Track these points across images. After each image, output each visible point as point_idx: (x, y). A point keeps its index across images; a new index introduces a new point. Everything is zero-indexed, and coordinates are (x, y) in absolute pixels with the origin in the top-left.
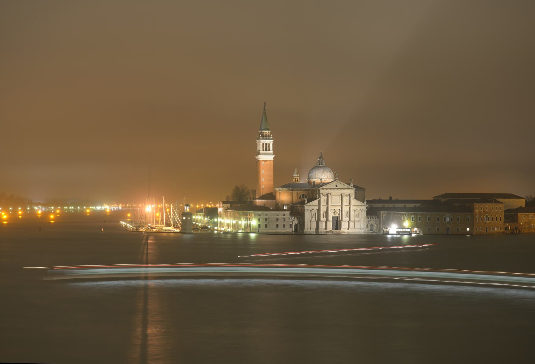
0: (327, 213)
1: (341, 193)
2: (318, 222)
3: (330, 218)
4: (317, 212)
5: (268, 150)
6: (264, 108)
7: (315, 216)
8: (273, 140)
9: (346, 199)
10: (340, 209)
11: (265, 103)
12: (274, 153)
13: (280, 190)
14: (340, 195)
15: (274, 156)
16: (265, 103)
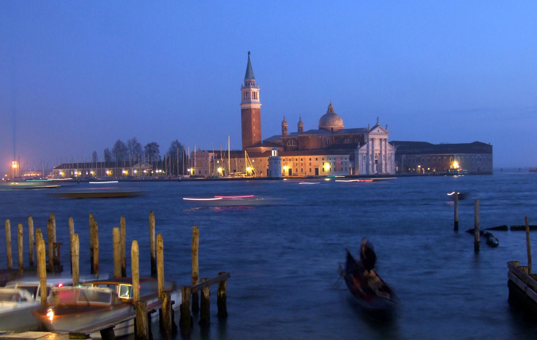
0: (372, 155)
1: (381, 138)
2: (367, 165)
3: (375, 162)
4: (365, 156)
5: (256, 98)
6: (249, 57)
7: (365, 159)
8: (259, 89)
9: (383, 143)
10: (379, 152)
11: (249, 53)
12: (261, 102)
13: (309, 136)
14: (379, 139)
16: (249, 53)
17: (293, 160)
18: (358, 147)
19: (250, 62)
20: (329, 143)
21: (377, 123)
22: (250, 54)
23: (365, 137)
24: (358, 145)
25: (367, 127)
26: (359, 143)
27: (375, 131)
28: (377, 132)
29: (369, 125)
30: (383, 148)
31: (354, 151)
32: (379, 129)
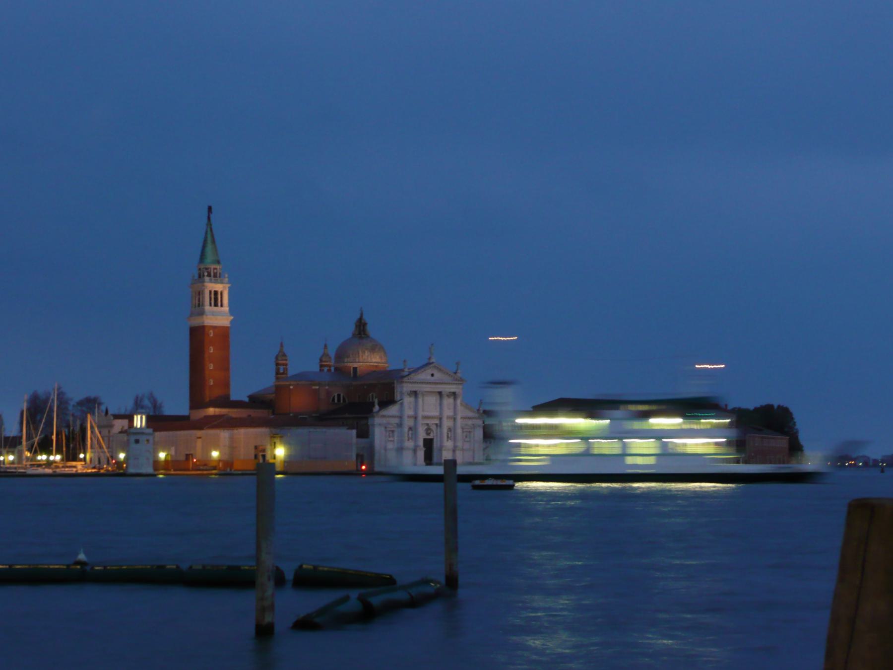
3: (421, 443)
5: (219, 304)
6: (209, 218)
7: (393, 436)
8: (229, 285)
11: (210, 208)
12: (232, 311)
15: (232, 317)
16: (210, 208)
20: (342, 401)
22: (213, 210)
25: (401, 367)
26: (376, 401)
27: (425, 375)
28: (429, 377)
30: (448, 412)
31: (367, 418)
32: (435, 372)
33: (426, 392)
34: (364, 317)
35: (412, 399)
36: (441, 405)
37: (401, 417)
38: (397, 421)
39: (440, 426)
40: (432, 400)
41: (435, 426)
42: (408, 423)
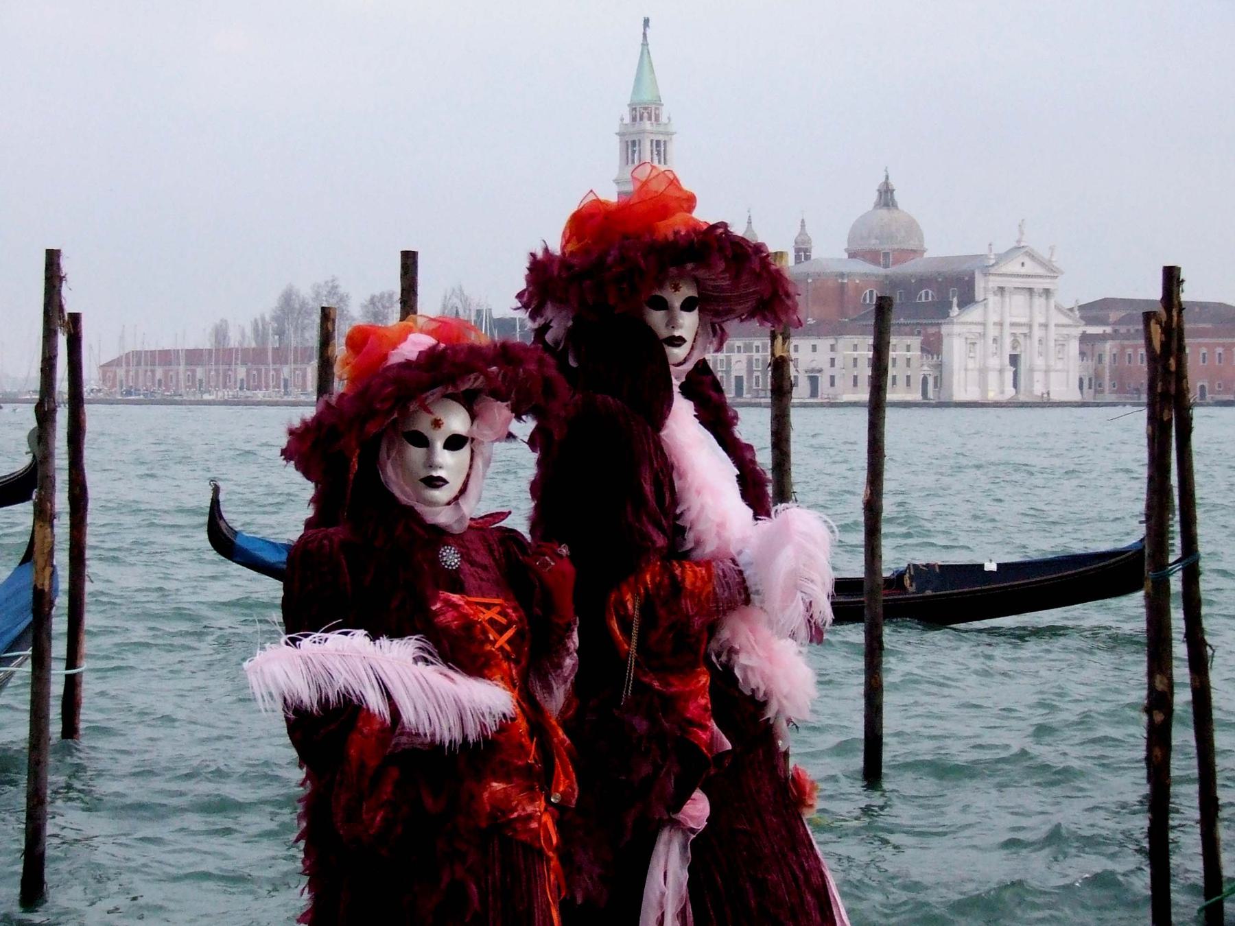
3: (1007, 361)
6: (645, 35)
7: (975, 352)
11: (646, 22)
16: (646, 22)
17: (748, 348)
18: (951, 315)
19: (648, 52)
21: (1019, 241)
22: (650, 24)
23: (980, 284)
24: (951, 307)
26: (955, 300)
27: (1013, 267)
29: (990, 245)
31: (939, 325)
33: (1015, 288)
34: (891, 181)
35: (998, 298)
36: (1031, 307)
37: (984, 325)
38: (979, 329)
39: (1030, 337)
40: (1020, 300)
41: (1022, 337)
42: (992, 332)
